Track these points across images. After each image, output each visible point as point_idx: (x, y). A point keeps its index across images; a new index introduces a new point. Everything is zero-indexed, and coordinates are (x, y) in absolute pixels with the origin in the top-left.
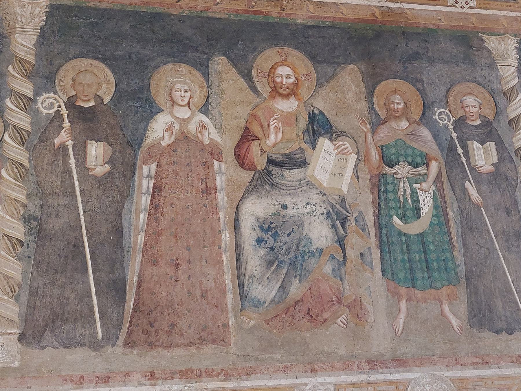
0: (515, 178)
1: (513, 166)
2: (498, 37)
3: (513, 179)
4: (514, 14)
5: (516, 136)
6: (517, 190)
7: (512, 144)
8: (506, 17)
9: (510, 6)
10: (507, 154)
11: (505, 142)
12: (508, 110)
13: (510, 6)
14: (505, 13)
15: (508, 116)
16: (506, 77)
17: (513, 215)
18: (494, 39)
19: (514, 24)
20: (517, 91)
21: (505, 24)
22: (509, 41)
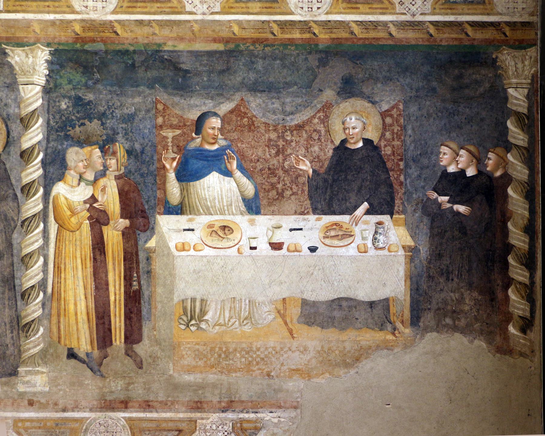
0: (16, 218)
1: (16, 204)
2: (26, 48)
3: (13, 220)
4: (51, 17)
5: (26, 170)
6: (15, 232)
7: (20, 180)
8: (40, 21)
9: (48, 6)
10: (11, 191)
11: (12, 178)
12: (23, 139)
13: (48, 6)
14: (40, 16)
15: (20, 147)
16: (28, 99)
17: (5, 259)
18: (20, 52)
19: (50, 29)
20: (38, 116)
21: (38, 31)
22: (40, 52)
